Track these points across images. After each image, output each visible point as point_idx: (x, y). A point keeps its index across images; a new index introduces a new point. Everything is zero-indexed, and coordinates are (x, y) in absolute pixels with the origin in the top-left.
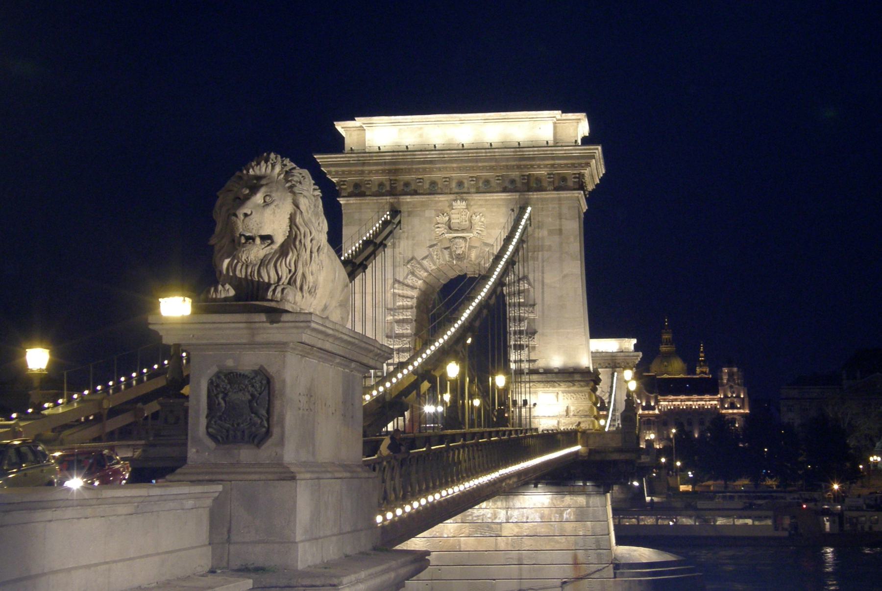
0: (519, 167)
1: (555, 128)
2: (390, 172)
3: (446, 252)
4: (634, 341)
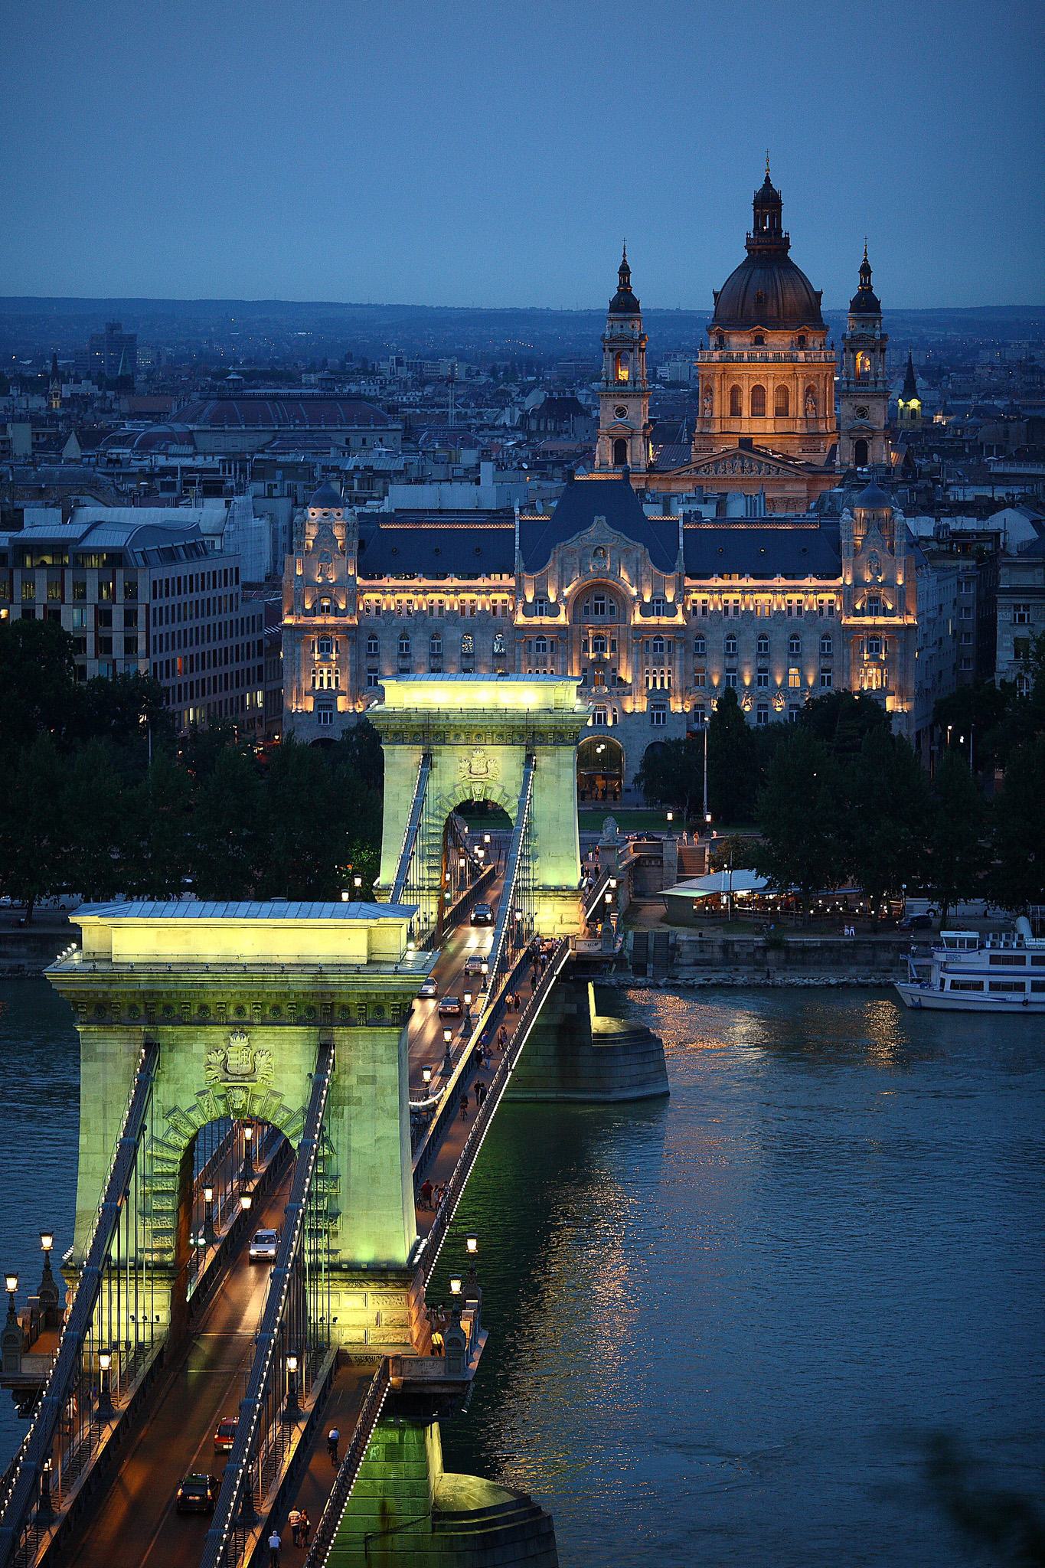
1: (370, 933)
3: (221, 1103)
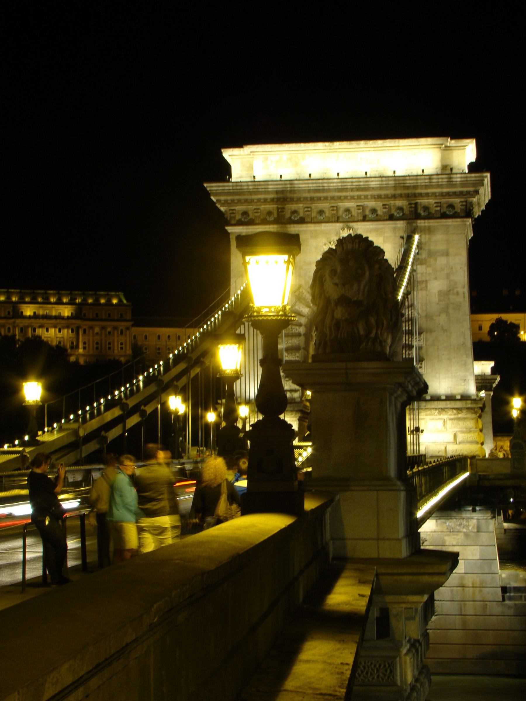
0: (407, 196)
2: (278, 200)
4: (492, 364)
